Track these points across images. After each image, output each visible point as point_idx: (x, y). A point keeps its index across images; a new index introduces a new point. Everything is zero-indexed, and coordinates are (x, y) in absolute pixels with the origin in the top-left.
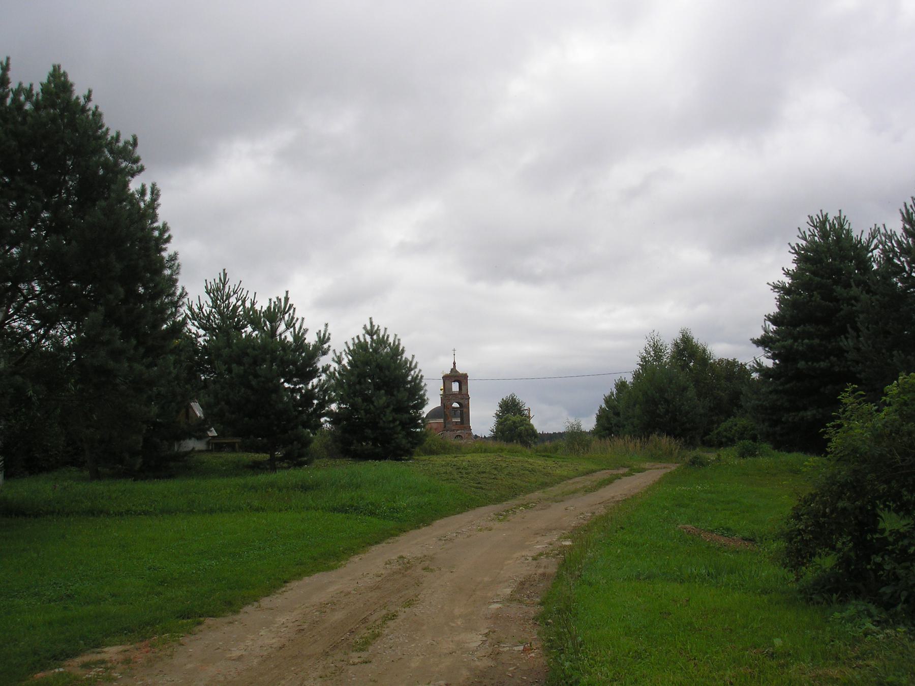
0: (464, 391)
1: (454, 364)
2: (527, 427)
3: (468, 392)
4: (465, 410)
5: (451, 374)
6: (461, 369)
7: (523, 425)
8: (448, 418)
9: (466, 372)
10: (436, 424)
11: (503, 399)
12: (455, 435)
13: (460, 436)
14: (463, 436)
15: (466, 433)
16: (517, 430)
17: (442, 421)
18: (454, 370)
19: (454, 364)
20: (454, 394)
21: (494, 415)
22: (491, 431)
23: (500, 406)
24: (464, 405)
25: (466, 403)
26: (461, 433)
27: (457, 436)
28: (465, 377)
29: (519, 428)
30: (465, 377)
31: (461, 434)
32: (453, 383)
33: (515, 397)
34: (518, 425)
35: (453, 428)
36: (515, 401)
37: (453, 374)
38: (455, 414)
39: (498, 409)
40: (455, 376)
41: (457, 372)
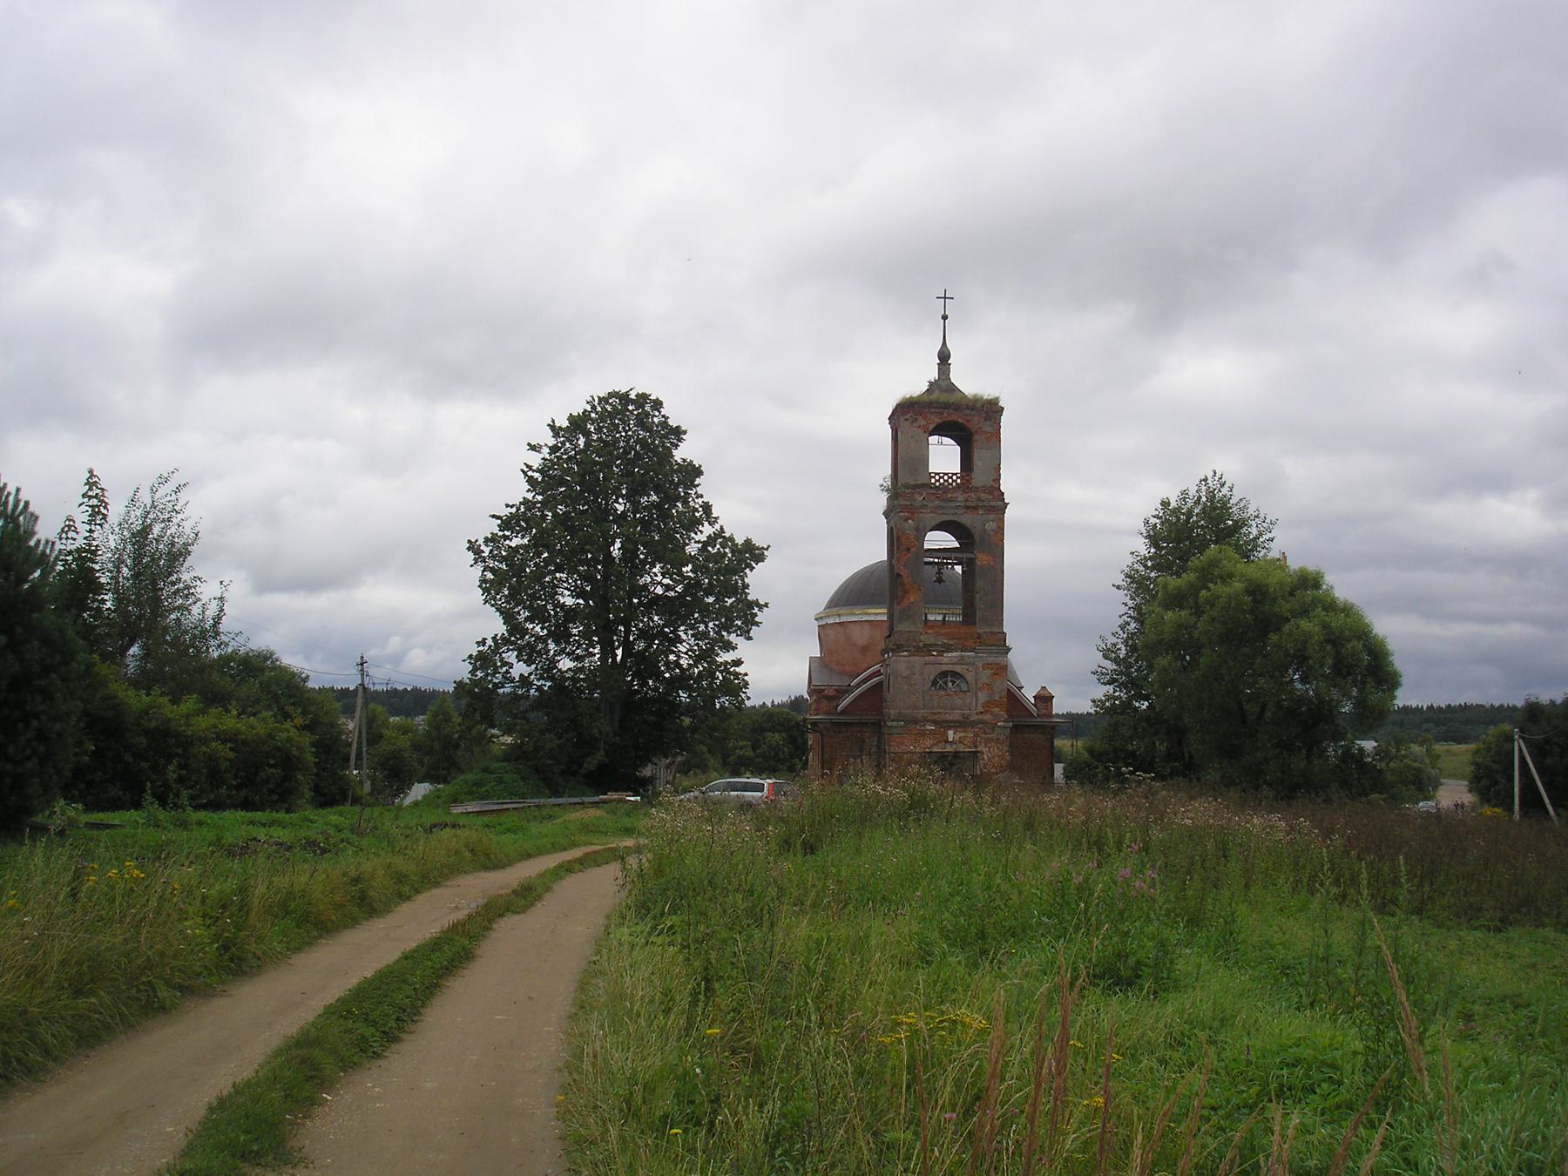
0: (980, 478)
1: (944, 357)
2: (1336, 621)
3: (998, 480)
4: (982, 559)
5: (925, 398)
6: (969, 381)
7: (1305, 612)
8: (906, 592)
9: (997, 396)
10: (867, 628)
11: (1165, 504)
12: (933, 671)
13: (955, 674)
14: (970, 677)
15: (987, 666)
16: (1273, 637)
17: (879, 614)
18: (943, 383)
19: (944, 357)
20: (940, 491)
21: (1120, 579)
22: (1105, 656)
23: (1154, 538)
24: (977, 532)
25: (990, 526)
26: (961, 661)
27: (944, 674)
28: (991, 410)
29: (1286, 628)
30: (991, 410)
31: (958, 668)
32: (933, 439)
33: (1225, 490)
34: (1284, 607)
35: (928, 638)
36: (1224, 504)
37: (934, 397)
38: (940, 580)
39: (1142, 547)
40: (947, 406)
41: (953, 389)
